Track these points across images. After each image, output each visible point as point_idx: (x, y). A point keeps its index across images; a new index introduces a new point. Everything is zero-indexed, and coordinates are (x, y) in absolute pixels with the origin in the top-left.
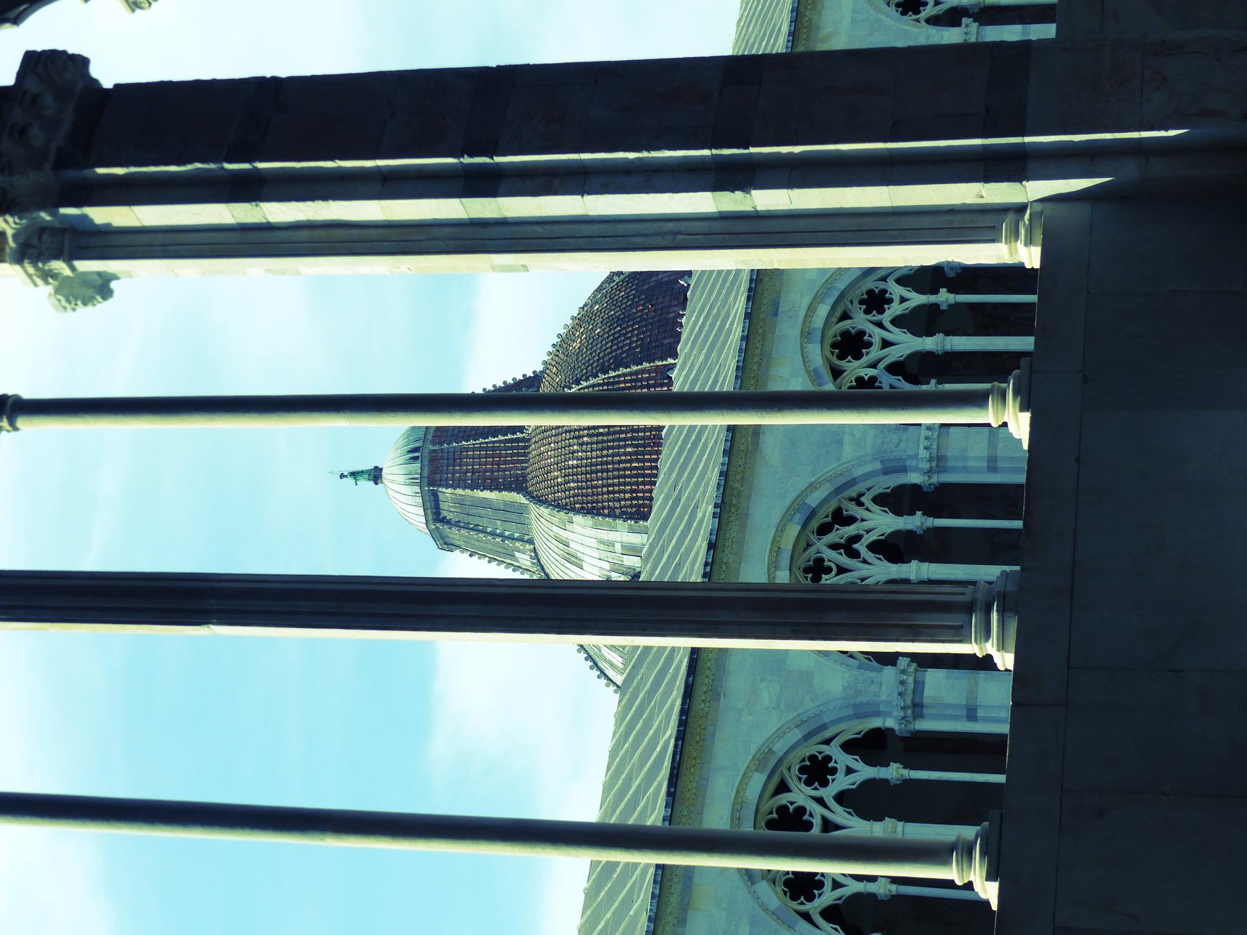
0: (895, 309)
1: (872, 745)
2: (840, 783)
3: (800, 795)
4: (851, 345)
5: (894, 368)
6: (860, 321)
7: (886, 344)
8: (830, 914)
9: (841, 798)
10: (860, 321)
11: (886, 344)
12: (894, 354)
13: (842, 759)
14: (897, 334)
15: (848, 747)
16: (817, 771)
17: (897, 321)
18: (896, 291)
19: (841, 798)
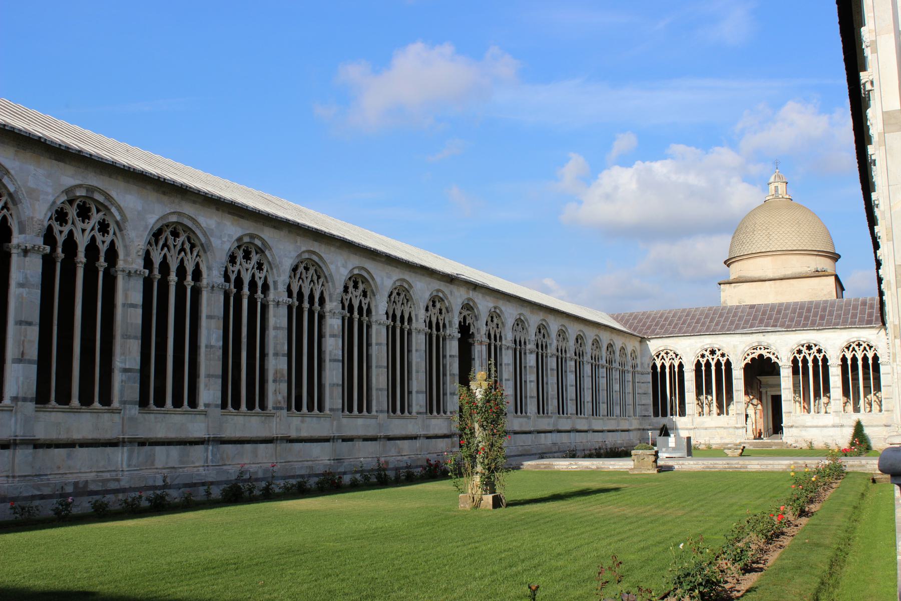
0: (818, 355)
1: (728, 364)
2: (721, 359)
3: (718, 353)
4: (809, 348)
5: (804, 357)
6: (815, 349)
7: (810, 354)
8: (698, 361)
9: (718, 360)
10: (815, 349)
11: (810, 354)
12: (807, 357)
13: (725, 359)
14: (812, 357)
15: (728, 359)
16: (723, 355)
17: (815, 356)
18: (822, 355)
19: (718, 360)
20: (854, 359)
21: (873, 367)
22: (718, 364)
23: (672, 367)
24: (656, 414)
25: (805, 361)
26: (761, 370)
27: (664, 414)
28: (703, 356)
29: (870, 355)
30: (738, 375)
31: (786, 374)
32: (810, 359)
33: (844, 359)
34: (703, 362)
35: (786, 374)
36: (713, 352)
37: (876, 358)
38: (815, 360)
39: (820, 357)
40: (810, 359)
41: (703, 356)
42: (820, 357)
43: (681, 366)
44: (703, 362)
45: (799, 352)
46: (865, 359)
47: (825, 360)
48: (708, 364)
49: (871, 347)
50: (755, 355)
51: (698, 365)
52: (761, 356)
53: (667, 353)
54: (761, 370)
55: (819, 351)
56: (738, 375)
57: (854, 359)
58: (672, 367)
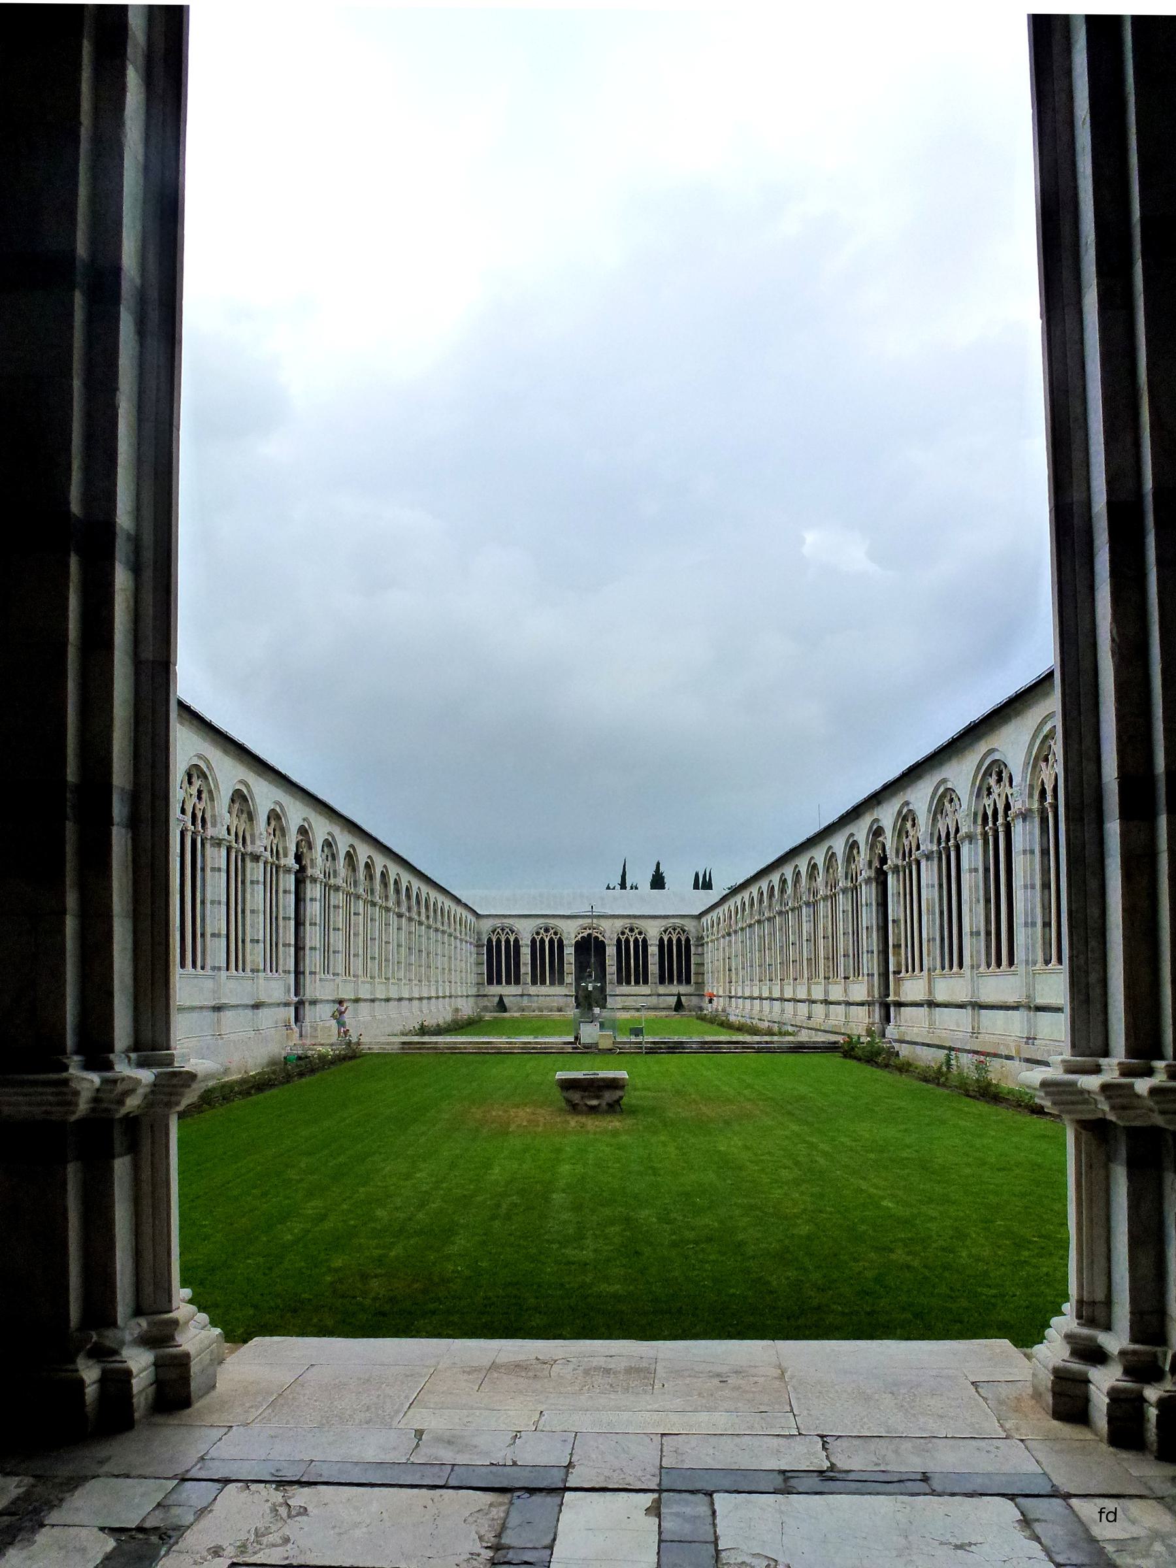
1: (560, 941)
4: (632, 930)
16: (556, 933)
20: (670, 940)
21: (685, 948)
22: (551, 941)
23: (507, 941)
24: (490, 982)
25: (627, 941)
26: (590, 948)
27: (499, 982)
28: (538, 933)
29: (683, 939)
30: (569, 951)
31: (611, 951)
32: (632, 940)
33: (661, 940)
34: (538, 938)
35: (611, 951)
36: (547, 930)
37: (688, 940)
38: (636, 940)
39: (640, 938)
40: (632, 940)
41: (538, 933)
42: (640, 938)
43: (516, 941)
44: (538, 938)
45: (623, 933)
46: (679, 940)
47: (645, 941)
48: (542, 941)
49: (684, 931)
50: (585, 934)
51: (533, 941)
52: (589, 935)
53: (503, 930)
54: (590, 948)
55: (640, 933)
56: (569, 951)
57: (670, 940)
58: (507, 941)
